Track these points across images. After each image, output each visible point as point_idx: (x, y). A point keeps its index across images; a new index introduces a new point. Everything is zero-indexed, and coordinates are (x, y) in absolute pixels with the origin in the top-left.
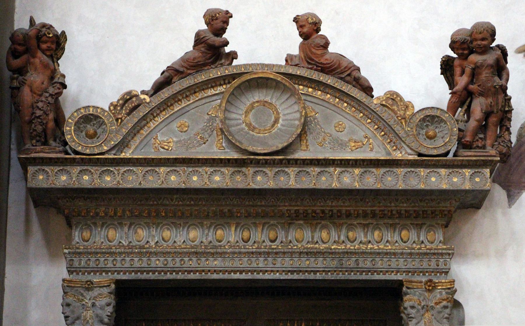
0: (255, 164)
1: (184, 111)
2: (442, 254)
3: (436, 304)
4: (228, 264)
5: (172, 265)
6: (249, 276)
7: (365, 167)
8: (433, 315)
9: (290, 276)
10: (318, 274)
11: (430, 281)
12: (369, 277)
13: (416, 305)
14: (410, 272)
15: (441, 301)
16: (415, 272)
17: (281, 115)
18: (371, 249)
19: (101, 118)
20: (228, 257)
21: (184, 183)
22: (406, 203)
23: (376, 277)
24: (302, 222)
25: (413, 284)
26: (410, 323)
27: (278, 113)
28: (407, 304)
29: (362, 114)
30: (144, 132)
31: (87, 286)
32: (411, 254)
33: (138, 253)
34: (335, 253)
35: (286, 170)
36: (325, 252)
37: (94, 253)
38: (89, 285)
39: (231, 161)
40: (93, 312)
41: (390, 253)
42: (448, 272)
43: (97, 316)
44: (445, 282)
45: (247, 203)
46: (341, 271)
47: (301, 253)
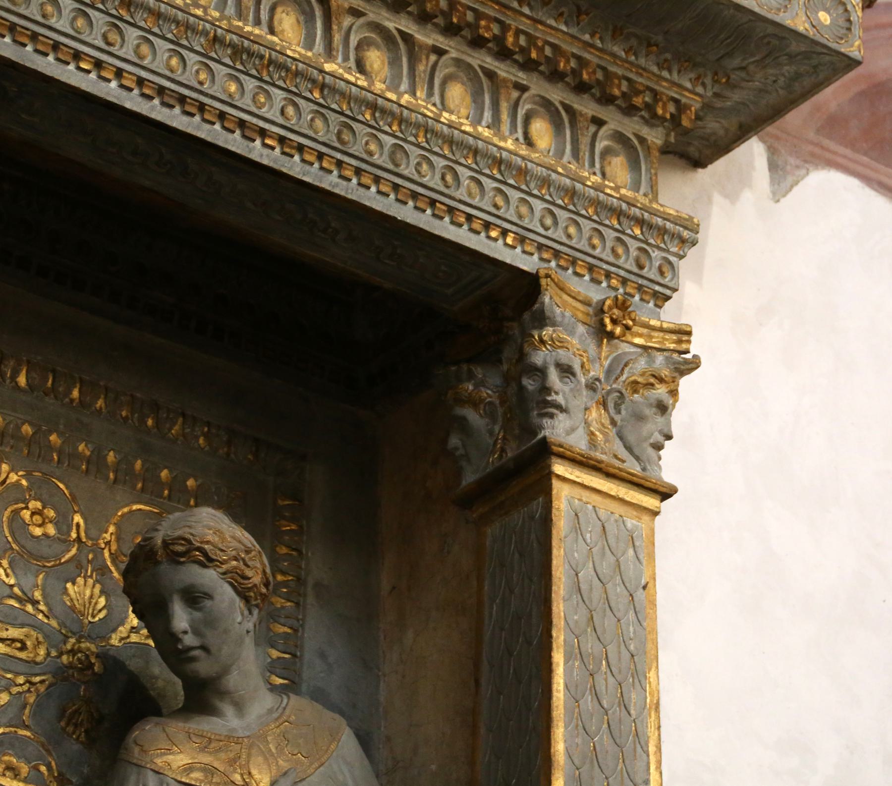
2: (662, 232)
11: (623, 305)
14: (557, 254)
15: (652, 380)
22: (566, 24)
25: (565, 297)
26: (546, 422)
32: (572, 193)
34: (334, 90)
36: (297, 73)
41: (509, 165)
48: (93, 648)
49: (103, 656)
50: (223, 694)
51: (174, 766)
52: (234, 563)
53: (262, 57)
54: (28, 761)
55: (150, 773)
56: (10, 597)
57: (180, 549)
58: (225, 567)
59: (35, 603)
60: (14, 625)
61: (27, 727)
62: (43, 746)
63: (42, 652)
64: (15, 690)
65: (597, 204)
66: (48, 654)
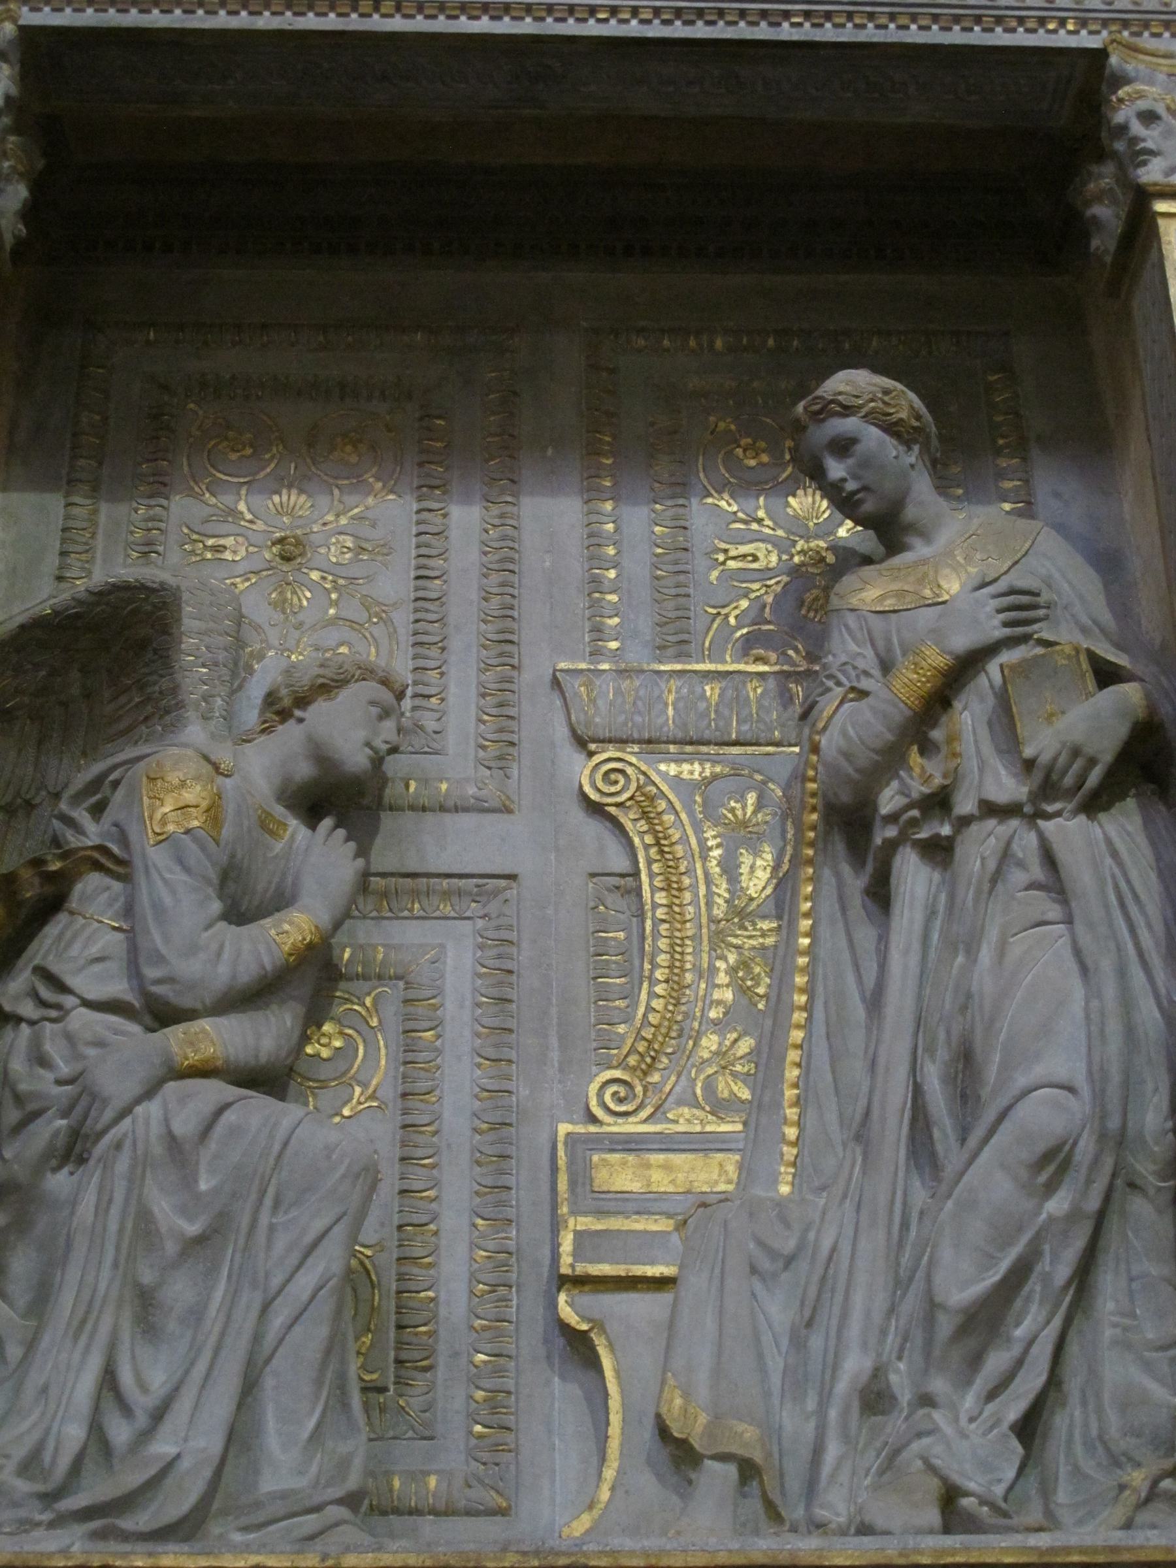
9: (678, 30)
10: (786, 25)
12: (977, 37)
13: (1160, 109)
16: (1146, 25)
23: (1000, 38)
26: (1141, 171)
28: (1119, 117)
46: (871, 16)
48: (822, 544)
49: (832, 548)
51: (868, 600)
52: (872, 404)
54: (775, 650)
55: (848, 613)
56: (735, 522)
57: (817, 407)
58: (864, 411)
59: (759, 521)
60: (742, 544)
61: (769, 623)
62: (787, 634)
63: (774, 559)
64: (753, 596)
66: (780, 559)
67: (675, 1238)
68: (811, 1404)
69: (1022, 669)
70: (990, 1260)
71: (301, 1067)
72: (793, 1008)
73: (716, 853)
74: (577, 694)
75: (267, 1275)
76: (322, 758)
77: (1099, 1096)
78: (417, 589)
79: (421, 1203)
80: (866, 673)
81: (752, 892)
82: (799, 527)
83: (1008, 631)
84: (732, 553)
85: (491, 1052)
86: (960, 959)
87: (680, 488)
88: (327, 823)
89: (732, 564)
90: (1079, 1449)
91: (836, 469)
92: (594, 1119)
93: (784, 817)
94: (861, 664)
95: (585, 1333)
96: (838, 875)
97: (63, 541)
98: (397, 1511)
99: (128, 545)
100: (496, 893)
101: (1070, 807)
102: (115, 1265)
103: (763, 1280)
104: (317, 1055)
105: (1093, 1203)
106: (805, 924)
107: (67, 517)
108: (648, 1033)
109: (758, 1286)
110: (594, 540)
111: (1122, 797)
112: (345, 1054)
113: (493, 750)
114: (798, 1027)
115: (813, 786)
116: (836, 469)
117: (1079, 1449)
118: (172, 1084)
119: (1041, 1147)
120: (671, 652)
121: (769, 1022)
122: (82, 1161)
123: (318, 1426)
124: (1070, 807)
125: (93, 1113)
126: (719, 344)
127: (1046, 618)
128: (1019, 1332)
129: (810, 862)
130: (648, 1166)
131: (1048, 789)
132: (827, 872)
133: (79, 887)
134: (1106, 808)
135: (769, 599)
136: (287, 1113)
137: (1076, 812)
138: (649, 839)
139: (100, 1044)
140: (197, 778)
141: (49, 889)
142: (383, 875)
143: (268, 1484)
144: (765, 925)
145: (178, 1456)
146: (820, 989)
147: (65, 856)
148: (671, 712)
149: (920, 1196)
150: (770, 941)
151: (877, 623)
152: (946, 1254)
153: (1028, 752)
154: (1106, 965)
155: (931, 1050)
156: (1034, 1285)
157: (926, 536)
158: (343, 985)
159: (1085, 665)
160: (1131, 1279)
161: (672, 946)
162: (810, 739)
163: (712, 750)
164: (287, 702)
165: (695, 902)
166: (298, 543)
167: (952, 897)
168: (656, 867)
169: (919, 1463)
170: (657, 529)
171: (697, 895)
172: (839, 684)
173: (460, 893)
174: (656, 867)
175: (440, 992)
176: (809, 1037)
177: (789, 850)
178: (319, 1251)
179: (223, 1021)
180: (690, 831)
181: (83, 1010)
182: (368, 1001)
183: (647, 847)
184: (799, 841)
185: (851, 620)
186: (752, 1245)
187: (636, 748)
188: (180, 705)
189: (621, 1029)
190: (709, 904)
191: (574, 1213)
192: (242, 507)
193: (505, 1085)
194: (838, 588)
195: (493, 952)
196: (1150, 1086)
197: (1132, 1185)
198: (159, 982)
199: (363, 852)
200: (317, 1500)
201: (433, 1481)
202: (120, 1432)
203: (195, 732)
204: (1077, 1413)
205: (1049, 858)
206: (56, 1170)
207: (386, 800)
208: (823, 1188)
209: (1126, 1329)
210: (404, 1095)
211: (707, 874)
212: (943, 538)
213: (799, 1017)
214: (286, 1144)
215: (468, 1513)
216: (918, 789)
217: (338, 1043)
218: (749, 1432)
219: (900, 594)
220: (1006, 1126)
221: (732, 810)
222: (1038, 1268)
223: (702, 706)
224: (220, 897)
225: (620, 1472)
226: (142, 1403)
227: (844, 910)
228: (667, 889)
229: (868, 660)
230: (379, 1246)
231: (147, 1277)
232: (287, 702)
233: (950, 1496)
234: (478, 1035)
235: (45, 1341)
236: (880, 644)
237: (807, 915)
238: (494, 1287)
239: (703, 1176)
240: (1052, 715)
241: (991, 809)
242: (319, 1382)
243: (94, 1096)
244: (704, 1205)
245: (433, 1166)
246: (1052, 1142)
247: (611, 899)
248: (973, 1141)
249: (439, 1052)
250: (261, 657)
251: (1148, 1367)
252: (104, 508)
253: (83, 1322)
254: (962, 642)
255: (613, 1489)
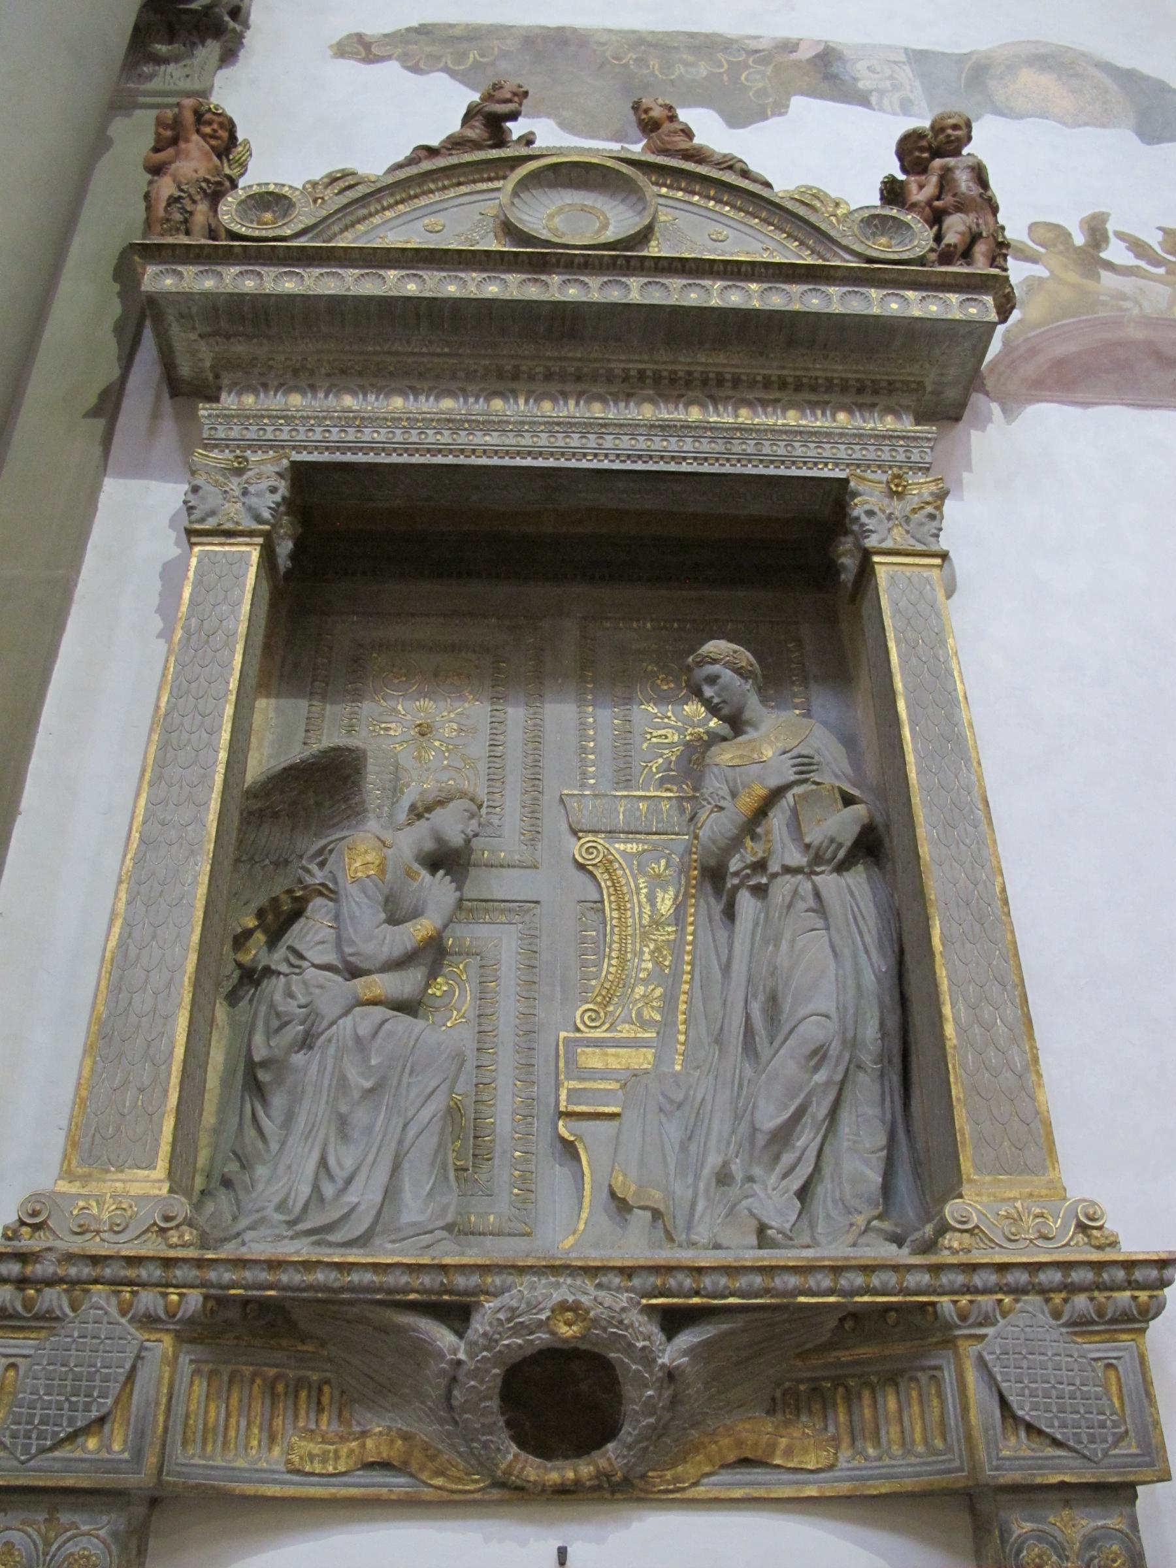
0: (566, 267)
1: (439, 207)
2: (916, 439)
3: (914, 511)
4: (511, 440)
5: (401, 440)
6: (551, 463)
7: (769, 281)
8: (908, 532)
9: (629, 466)
12: (782, 471)
13: (876, 509)
14: (858, 466)
16: (869, 466)
17: (612, 221)
18: (784, 425)
19: (285, 197)
20: (511, 431)
21: (430, 290)
23: (794, 472)
24: (651, 392)
26: (866, 541)
27: (606, 218)
28: (855, 513)
29: (757, 221)
30: (359, 227)
31: (236, 464)
32: (861, 436)
33: (339, 418)
34: (717, 429)
35: (624, 279)
37: (256, 416)
38: (240, 463)
39: (520, 259)
40: (244, 504)
42: (928, 469)
43: (250, 509)
44: (926, 483)
45: (548, 354)
46: (728, 460)
47: (652, 426)
48: (701, 730)
49: (707, 733)
50: (748, 723)
53: (675, 426)
59: (669, 718)
63: (676, 738)
65: (876, 436)
67: (620, 1092)
68: (690, 1180)
69: (804, 797)
70: (786, 1107)
71: (425, 1000)
72: (684, 973)
73: (644, 891)
74: (573, 807)
75: (406, 1109)
76: (439, 840)
77: (842, 1020)
78: (490, 751)
79: (488, 1073)
80: (724, 798)
81: (663, 911)
82: (689, 721)
83: (797, 777)
84: (655, 734)
85: (524, 994)
86: (771, 948)
87: (628, 700)
88: (441, 872)
89: (654, 740)
90: (829, 1203)
91: (708, 692)
92: (578, 1030)
93: (680, 873)
94: (721, 793)
95: (572, 1142)
96: (708, 904)
97: (307, 724)
98: (472, 1233)
99: (340, 726)
100: (529, 910)
101: (829, 868)
102: (327, 1103)
103: (666, 1115)
104: (434, 994)
105: (839, 1077)
106: (691, 929)
107: (309, 712)
108: (607, 985)
109: (663, 1119)
110: (583, 727)
111: (855, 864)
112: (449, 993)
113: (529, 836)
114: (686, 982)
115: (695, 856)
116: (708, 692)
117: (829, 1203)
118: (358, 1009)
119: (812, 1047)
120: (621, 785)
121: (670, 981)
122: (311, 1048)
123: (431, 1189)
124: (829, 868)
125: (317, 1023)
126: (649, 625)
127: (817, 770)
128: (799, 1144)
129: (693, 896)
130: (606, 1055)
131: (818, 859)
132: (702, 901)
133: (311, 905)
134: (847, 870)
135: (674, 758)
136: (418, 1025)
137: (831, 872)
138: (609, 883)
139: (321, 987)
140: (373, 849)
141: (296, 905)
142: (469, 900)
143: (406, 1218)
144: (670, 929)
145: (358, 1204)
146: (697, 962)
147: (305, 888)
148: (621, 817)
149: (749, 1072)
150: (672, 937)
151: (729, 771)
152: (762, 1103)
153: (807, 840)
154: (847, 952)
155: (755, 996)
156: (807, 1119)
157: (755, 727)
158: (448, 957)
159: (837, 795)
160: (858, 1116)
161: (621, 939)
162: (694, 832)
163: (642, 837)
164: (421, 809)
165: (633, 916)
166: (429, 726)
167: (767, 914)
168: (613, 898)
169: (746, 1212)
170: (616, 721)
171: (633, 913)
172: (709, 803)
173: (510, 911)
174: (613, 898)
175: (498, 962)
176: (691, 988)
177: (682, 890)
178: (433, 1097)
179: (385, 976)
180: (631, 880)
181: (313, 969)
182: (461, 966)
183: (608, 887)
184: (688, 886)
185: (716, 770)
186: (661, 1097)
187: (603, 835)
188: (365, 810)
189: (593, 982)
190: (640, 917)
191: (568, 1078)
192: (400, 707)
193: (532, 1011)
194: (709, 753)
195: (526, 942)
196: (869, 1015)
197: (859, 1067)
198: (351, 955)
199: (459, 888)
200: (430, 1227)
201: (492, 1218)
202: (329, 1190)
203: (372, 824)
204: (829, 1186)
205: (818, 895)
206: (298, 1051)
207: (472, 861)
208: (698, 1067)
209: (855, 1142)
210: (479, 1016)
211: (639, 902)
212: (763, 728)
213: (687, 977)
214: (417, 1040)
215: (510, 1235)
216: (750, 859)
217: (445, 988)
218: (657, 1195)
219: (742, 757)
220: (794, 1036)
221: (653, 869)
222: (810, 1110)
223: (638, 813)
224: (385, 911)
225: (590, 1214)
226: (340, 1175)
227: (711, 921)
228: (618, 909)
229: (725, 791)
230: (465, 1095)
231: (343, 1109)
232: (421, 809)
233: (762, 1229)
234: (518, 985)
235: (290, 1142)
236: (731, 784)
237: (691, 924)
238: (525, 1117)
239: (635, 1060)
240: (820, 821)
241: (787, 870)
242: (433, 1164)
243: (317, 1015)
244: (635, 1075)
245: (494, 1054)
246: (818, 1044)
247: (589, 914)
248: (776, 1044)
249: (497, 993)
250: (408, 786)
251: (866, 1162)
252: (328, 707)
253: (310, 1132)
254: (774, 782)
255: (586, 1223)
